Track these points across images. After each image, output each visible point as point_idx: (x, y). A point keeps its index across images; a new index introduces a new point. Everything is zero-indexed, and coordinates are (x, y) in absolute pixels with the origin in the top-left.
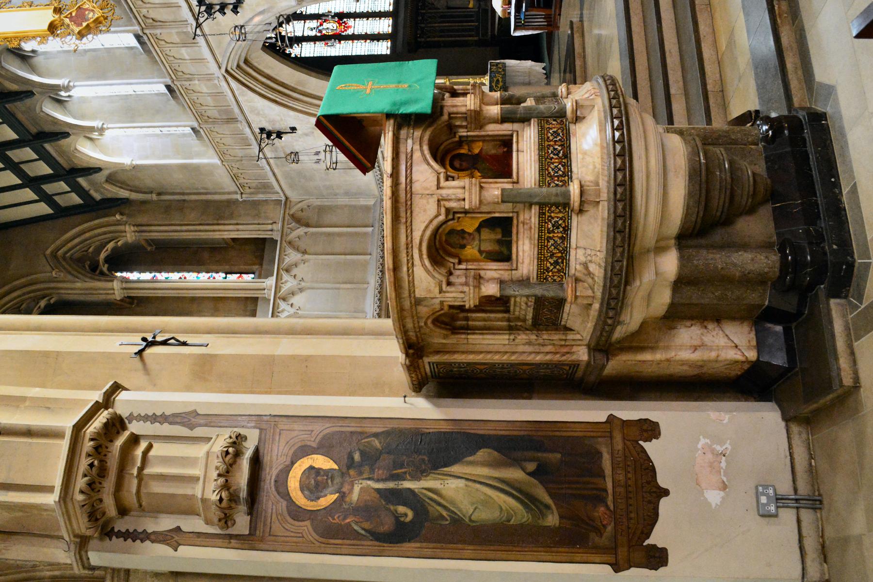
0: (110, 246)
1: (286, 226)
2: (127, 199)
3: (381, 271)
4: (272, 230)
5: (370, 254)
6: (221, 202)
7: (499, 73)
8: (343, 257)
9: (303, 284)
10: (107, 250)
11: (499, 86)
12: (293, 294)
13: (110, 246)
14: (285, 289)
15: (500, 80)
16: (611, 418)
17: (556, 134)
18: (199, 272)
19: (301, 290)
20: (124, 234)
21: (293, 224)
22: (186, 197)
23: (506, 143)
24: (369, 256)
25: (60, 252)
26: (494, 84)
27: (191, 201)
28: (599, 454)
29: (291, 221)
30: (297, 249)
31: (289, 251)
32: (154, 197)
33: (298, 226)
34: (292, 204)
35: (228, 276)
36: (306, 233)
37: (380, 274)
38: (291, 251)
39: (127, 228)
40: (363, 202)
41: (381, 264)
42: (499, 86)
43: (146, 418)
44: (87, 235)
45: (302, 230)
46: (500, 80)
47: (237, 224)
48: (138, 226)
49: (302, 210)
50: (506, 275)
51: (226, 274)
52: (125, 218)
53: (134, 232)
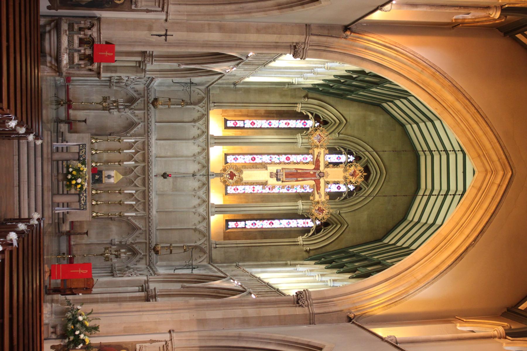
0: (310, 234)
1: (208, 246)
2: (305, 261)
3: (150, 218)
4: (216, 244)
5: (157, 230)
6: (249, 261)
7: (83, 205)
8: (173, 228)
9: (194, 210)
10: (312, 230)
11: (82, 198)
12: (199, 205)
13: (310, 234)
14: (204, 207)
15: (82, 201)
16: (57, 10)
17: (71, 46)
18: (262, 228)
19: (195, 207)
20: (303, 240)
21: (204, 247)
22: (270, 263)
23: (80, 46)
24: (157, 228)
25: (339, 226)
26: (85, 199)
27: (266, 261)
28: (60, 3)
29: (205, 249)
30: (200, 232)
31: (202, 229)
32: (289, 262)
33: (200, 246)
34: (205, 260)
35: (244, 226)
36: (196, 242)
37: (150, 216)
38: (203, 230)
39: (301, 242)
40: (164, 263)
41: (150, 222)
42: (82, 198)
43: (158, 11)
44: (325, 238)
45: (199, 243)
46: (82, 201)
47: (237, 247)
48: (296, 245)
49: (200, 257)
50: (80, 25)
51: (245, 227)
52: (304, 249)
53: (298, 242)
